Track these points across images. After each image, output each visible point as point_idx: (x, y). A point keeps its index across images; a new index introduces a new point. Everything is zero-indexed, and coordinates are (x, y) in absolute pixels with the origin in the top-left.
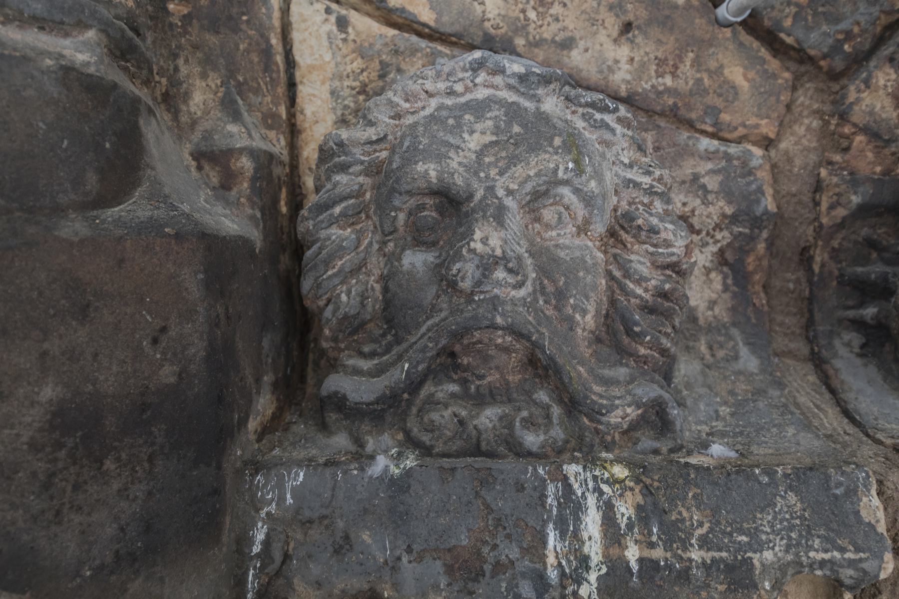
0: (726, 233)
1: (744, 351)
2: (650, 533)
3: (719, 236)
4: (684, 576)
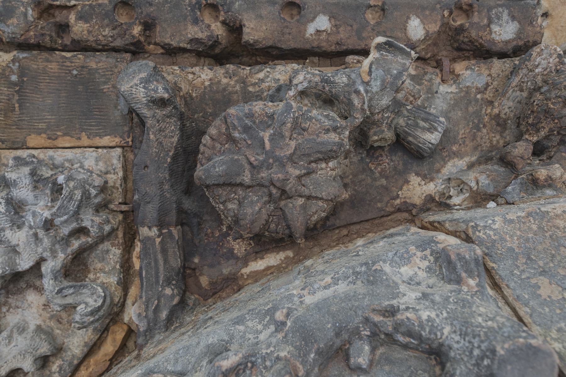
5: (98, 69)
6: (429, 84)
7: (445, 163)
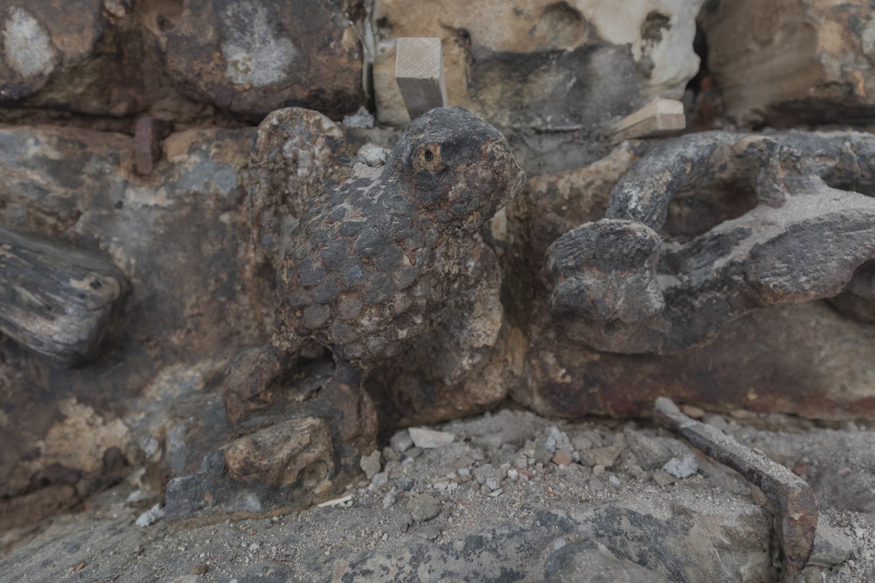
6: (97, 184)
7: (154, 374)
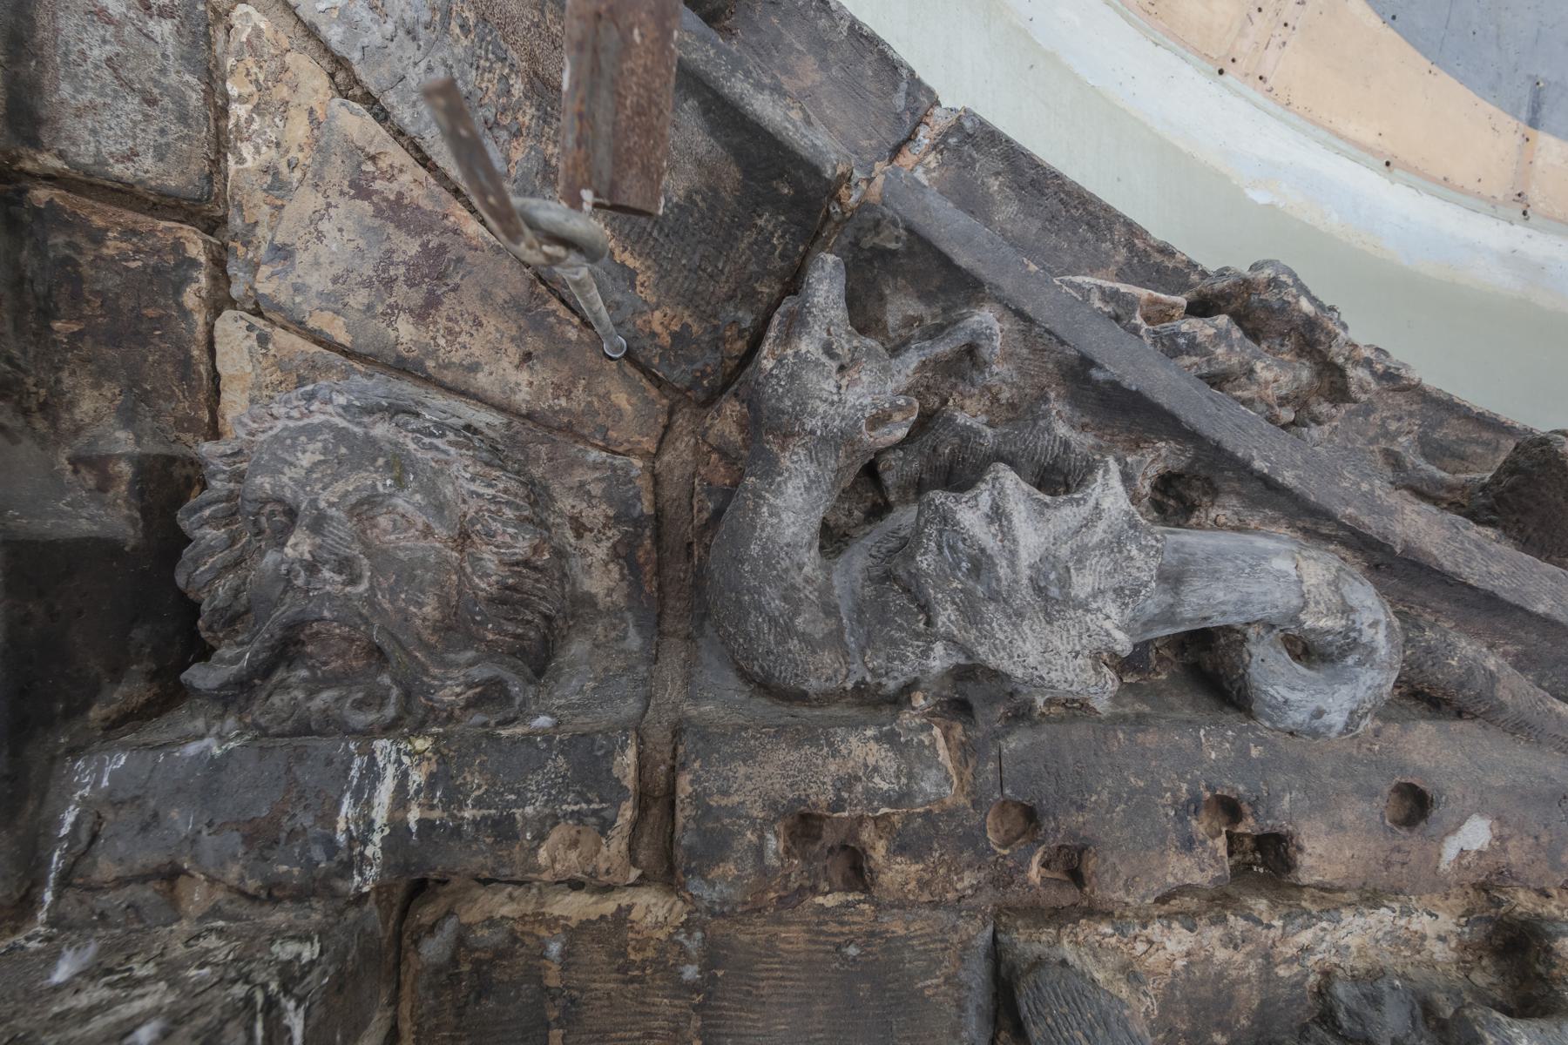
0: (614, 531)
1: (632, 632)
2: (433, 797)
3: (610, 534)
4: (457, 832)
5: (912, 938)
